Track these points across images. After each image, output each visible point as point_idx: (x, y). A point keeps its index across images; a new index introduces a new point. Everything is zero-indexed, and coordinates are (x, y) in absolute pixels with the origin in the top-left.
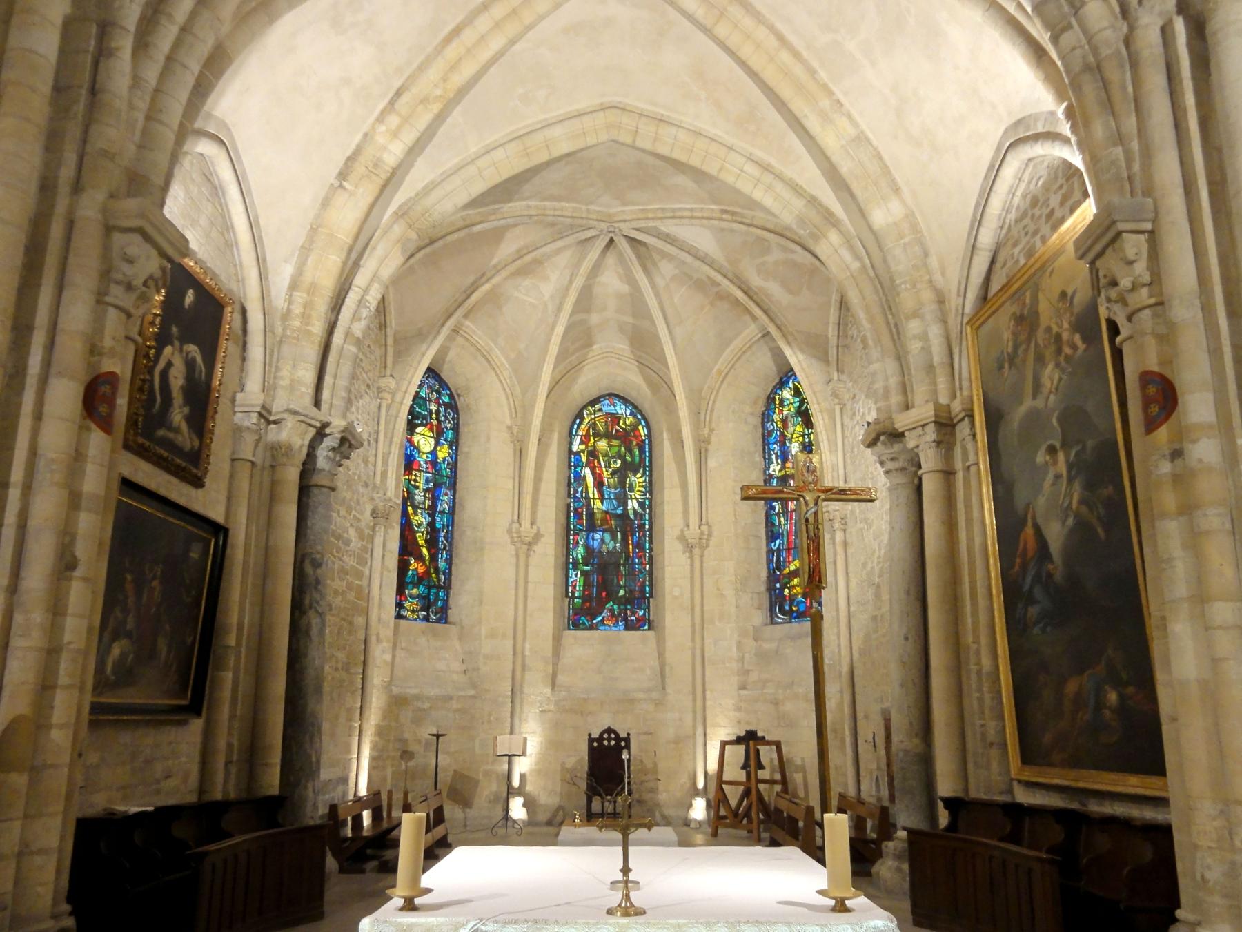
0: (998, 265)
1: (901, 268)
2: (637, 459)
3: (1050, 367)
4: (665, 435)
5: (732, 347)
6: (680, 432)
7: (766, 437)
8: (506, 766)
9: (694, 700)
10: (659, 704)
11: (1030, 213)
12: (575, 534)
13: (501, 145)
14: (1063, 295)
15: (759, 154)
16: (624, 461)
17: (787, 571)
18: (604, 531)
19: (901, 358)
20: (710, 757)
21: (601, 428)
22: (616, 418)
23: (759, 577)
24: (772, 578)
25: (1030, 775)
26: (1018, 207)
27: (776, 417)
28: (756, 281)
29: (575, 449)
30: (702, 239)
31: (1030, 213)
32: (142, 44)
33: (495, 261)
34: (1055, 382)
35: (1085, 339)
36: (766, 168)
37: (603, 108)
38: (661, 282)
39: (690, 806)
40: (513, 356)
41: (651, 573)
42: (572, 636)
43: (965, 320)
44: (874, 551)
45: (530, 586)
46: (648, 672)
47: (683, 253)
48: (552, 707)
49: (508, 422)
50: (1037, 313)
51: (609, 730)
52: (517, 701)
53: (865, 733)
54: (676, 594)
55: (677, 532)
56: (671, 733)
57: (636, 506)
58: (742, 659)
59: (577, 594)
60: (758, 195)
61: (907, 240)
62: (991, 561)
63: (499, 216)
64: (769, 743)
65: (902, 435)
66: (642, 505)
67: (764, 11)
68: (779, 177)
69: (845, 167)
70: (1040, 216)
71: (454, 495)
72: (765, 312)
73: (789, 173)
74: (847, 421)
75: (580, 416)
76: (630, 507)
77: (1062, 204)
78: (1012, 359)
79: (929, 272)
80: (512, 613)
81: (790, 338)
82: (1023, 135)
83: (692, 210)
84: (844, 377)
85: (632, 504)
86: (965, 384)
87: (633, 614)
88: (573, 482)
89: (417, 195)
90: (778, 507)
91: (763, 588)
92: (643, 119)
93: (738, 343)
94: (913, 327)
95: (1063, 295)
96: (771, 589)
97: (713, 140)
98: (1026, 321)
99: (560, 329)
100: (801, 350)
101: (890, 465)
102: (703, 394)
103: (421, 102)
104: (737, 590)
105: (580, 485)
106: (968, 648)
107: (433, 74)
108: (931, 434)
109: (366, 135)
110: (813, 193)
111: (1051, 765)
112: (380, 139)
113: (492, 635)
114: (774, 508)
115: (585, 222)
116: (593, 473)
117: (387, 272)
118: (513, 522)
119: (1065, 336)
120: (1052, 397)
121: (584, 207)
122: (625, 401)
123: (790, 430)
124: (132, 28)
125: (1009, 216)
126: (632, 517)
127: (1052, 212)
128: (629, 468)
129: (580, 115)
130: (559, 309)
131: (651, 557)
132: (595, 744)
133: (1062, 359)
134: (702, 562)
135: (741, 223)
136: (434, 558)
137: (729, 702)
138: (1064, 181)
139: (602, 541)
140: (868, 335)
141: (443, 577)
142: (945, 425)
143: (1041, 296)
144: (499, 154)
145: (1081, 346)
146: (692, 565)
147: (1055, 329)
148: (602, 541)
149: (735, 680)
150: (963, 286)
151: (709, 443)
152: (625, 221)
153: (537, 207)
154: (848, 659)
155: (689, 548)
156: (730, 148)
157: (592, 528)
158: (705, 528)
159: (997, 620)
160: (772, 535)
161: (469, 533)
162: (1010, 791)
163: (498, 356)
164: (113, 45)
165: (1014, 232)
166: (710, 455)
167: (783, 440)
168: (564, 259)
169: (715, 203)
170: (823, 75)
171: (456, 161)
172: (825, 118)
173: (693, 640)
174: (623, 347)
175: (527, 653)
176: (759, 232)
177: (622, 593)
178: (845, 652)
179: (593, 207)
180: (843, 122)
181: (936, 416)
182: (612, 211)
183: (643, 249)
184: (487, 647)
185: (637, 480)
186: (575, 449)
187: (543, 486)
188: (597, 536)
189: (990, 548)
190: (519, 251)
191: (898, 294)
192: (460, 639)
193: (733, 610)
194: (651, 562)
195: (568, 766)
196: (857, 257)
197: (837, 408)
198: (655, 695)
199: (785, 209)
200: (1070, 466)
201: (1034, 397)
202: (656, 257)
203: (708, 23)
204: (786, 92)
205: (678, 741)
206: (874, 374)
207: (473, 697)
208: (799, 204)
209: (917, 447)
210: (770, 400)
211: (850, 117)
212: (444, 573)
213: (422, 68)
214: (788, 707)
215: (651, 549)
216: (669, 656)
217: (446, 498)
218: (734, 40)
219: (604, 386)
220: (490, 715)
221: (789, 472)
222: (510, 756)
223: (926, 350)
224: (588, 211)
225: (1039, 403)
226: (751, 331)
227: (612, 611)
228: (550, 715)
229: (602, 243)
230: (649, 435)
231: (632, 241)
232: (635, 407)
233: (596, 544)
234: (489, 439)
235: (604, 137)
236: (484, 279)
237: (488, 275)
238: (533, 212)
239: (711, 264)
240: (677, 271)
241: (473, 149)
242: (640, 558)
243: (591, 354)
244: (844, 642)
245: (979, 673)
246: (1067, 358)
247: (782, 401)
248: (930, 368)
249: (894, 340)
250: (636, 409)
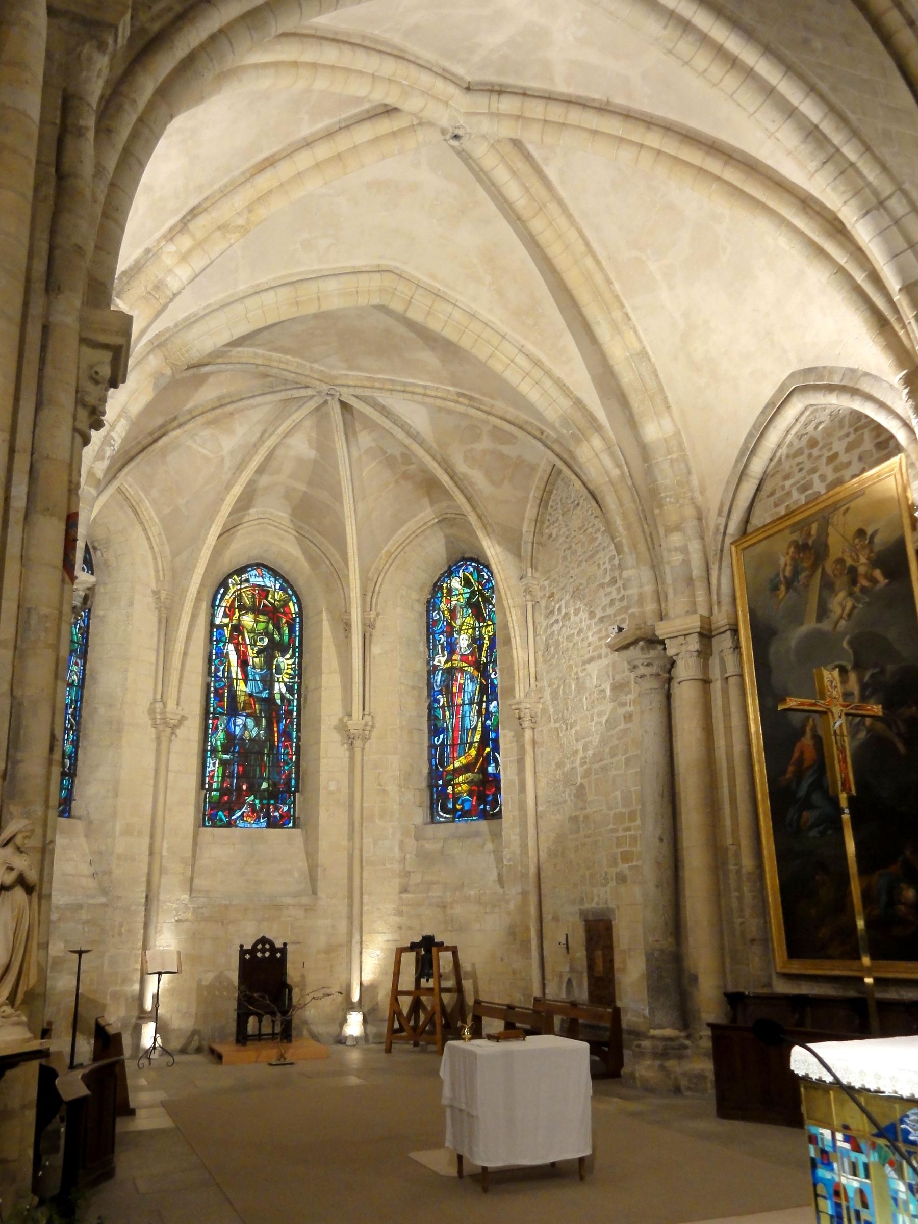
0: (763, 494)
1: (668, 482)
2: (286, 638)
3: (842, 595)
4: (325, 615)
5: (404, 529)
6: (348, 612)
7: (430, 626)
8: (137, 987)
9: (351, 906)
10: (309, 909)
11: (807, 452)
12: (215, 718)
13: (272, 288)
14: (861, 533)
15: (531, 348)
16: (272, 640)
17: (451, 767)
18: (247, 716)
19: (656, 566)
20: (372, 963)
22: (264, 592)
23: (420, 772)
24: (434, 775)
25: (796, 967)
26: (791, 445)
27: (443, 606)
28: (462, 467)
29: (218, 621)
30: (417, 416)
31: (807, 452)
32: (104, 130)
33: (190, 405)
34: (848, 609)
35: (886, 575)
36: (537, 363)
37: (380, 271)
38: (355, 453)
39: (345, 1020)
40: (167, 511)
41: (298, 764)
42: (208, 833)
43: (728, 540)
44: (576, 752)
45: (171, 776)
46: (296, 875)
47: (396, 428)
48: (189, 915)
49: (153, 585)
50: (826, 546)
51: (263, 940)
52: (154, 908)
53: (556, 935)
54: (332, 787)
55: (334, 721)
56: (321, 941)
57: (284, 690)
58: (403, 860)
59: (215, 786)
60: (525, 388)
61: (674, 456)
62: (757, 768)
63: (226, 360)
64: (447, 949)
65: (662, 642)
66: (290, 689)
67: (577, 215)
68: (548, 373)
69: (627, 377)
70: (819, 457)
71: (84, 665)
72: (469, 499)
73: (558, 372)
74: (540, 619)
75: (224, 584)
76: (276, 690)
77: (848, 450)
78: (790, 584)
79: (691, 490)
81: (490, 530)
82: (810, 381)
83: (425, 387)
84: (537, 575)
85: (279, 688)
86: (726, 600)
87: (277, 809)
88: (214, 659)
89: (176, 326)
90: (442, 700)
91: (424, 784)
92: (421, 291)
93: (411, 525)
95: (861, 533)
96: (431, 786)
97: (487, 325)
98: (810, 551)
99: (237, 490)
100: (499, 543)
101: (642, 670)
102: (370, 575)
103: (219, 228)
104: (400, 786)
105: (222, 663)
106: (727, 849)
107: (239, 200)
108: (694, 644)
109: (148, 251)
110: (579, 395)
111: (830, 958)
112: (168, 260)
113: (128, 831)
114: (438, 701)
116: (237, 650)
117: (135, 408)
118: (155, 701)
119: (862, 570)
120: (843, 623)
121: (308, 364)
122: (275, 573)
123: (459, 621)
124: (95, 106)
125: (780, 451)
126: (279, 702)
127: (833, 458)
130: (240, 468)
131: (298, 747)
132: (248, 956)
133: (857, 589)
134: (362, 756)
135: (478, 409)
137: (389, 907)
138: (851, 430)
139: (245, 726)
140: (624, 541)
141: (68, 762)
142: (706, 635)
143: (831, 530)
144: (269, 298)
145: (883, 581)
146: (352, 758)
147: (849, 562)
148: (245, 726)
149: (396, 883)
150: (726, 509)
151: (374, 628)
152: (348, 386)
153: (263, 356)
154: (536, 860)
155: (350, 740)
156: (504, 337)
157: (233, 711)
158: (368, 718)
159: (762, 823)
160: (435, 729)
161: (102, 711)
162: (769, 985)
163: (147, 508)
164: (82, 123)
165: (786, 466)
166: (374, 639)
167: (450, 631)
169: (454, 385)
170: (617, 286)
171: (222, 296)
172: (616, 329)
173: (351, 838)
174: (283, 515)
175: (164, 853)
176: (498, 422)
177: (265, 786)
178: (532, 853)
179: (316, 366)
180: (630, 336)
181: (701, 627)
182: (334, 373)
183: (348, 416)
184: (120, 848)
185: (285, 662)
186: (218, 621)
187: (189, 661)
188: (240, 721)
189: (755, 756)
190: (220, 398)
191: (661, 507)
192: (86, 836)
193: (396, 807)
194: (298, 753)
195: (204, 983)
196: (618, 466)
197: (529, 605)
198: (305, 900)
199: (551, 407)
200: (863, 687)
201: (819, 619)
202: (358, 426)
203: (526, 214)
204: (584, 296)
205: (330, 950)
206: (628, 580)
207: (105, 905)
208: (565, 404)
209: (677, 655)
210: (437, 587)
211: (636, 332)
212: (70, 758)
213: (226, 192)
214: (458, 910)
215: (298, 738)
216: (324, 857)
217: (75, 668)
218: (546, 237)
219: (255, 554)
220: (121, 925)
221: (456, 664)
223: (686, 563)
224: (312, 368)
225: (826, 626)
226: (427, 513)
227: (253, 806)
228: (187, 924)
229: (312, 405)
230: (300, 613)
231: (344, 405)
232: (285, 581)
233: (238, 731)
234: (131, 604)
235: (376, 301)
236: (175, 424)
237: (182, 419)
238: (260, 361)
239: (422, 443)
240: (373, 444)
241: (242, 287)
242: (286, 747)
243: (246, 520)
244: (531, 842)
245: (738, 872)
246: (864, 590)
247: (450, 590)
248: (690, 581)
249: (649, 549)
250: (287, 584)
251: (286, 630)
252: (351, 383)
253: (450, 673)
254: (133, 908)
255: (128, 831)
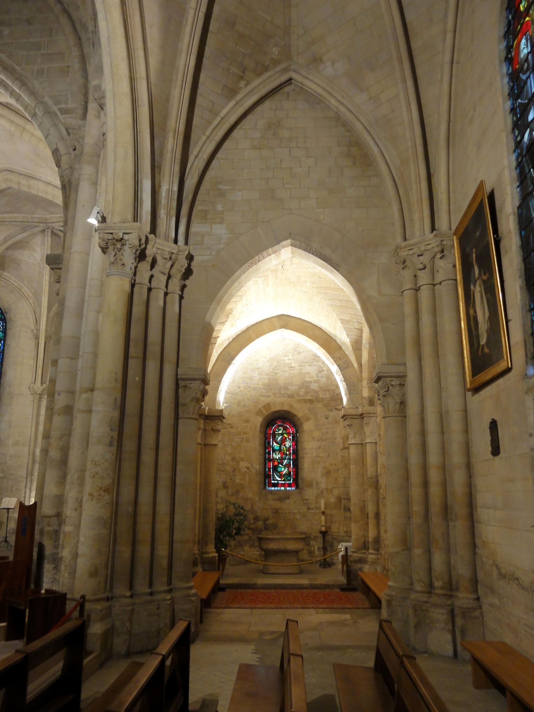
40: (33, 291)
80: (30, 432)
113: (16, 444)
115: (30, 224)
118: (32, 383)
152: (53, 222)
161: (7, 389)
168: (38, 240)
182: (48, 217)
190: (5, 238)
220: (12, 487)
222: (8, 509)
224: (32, 218)
234: (19, 337)
252: (55, 221)
254: (19, 479)
255: (16, 444)
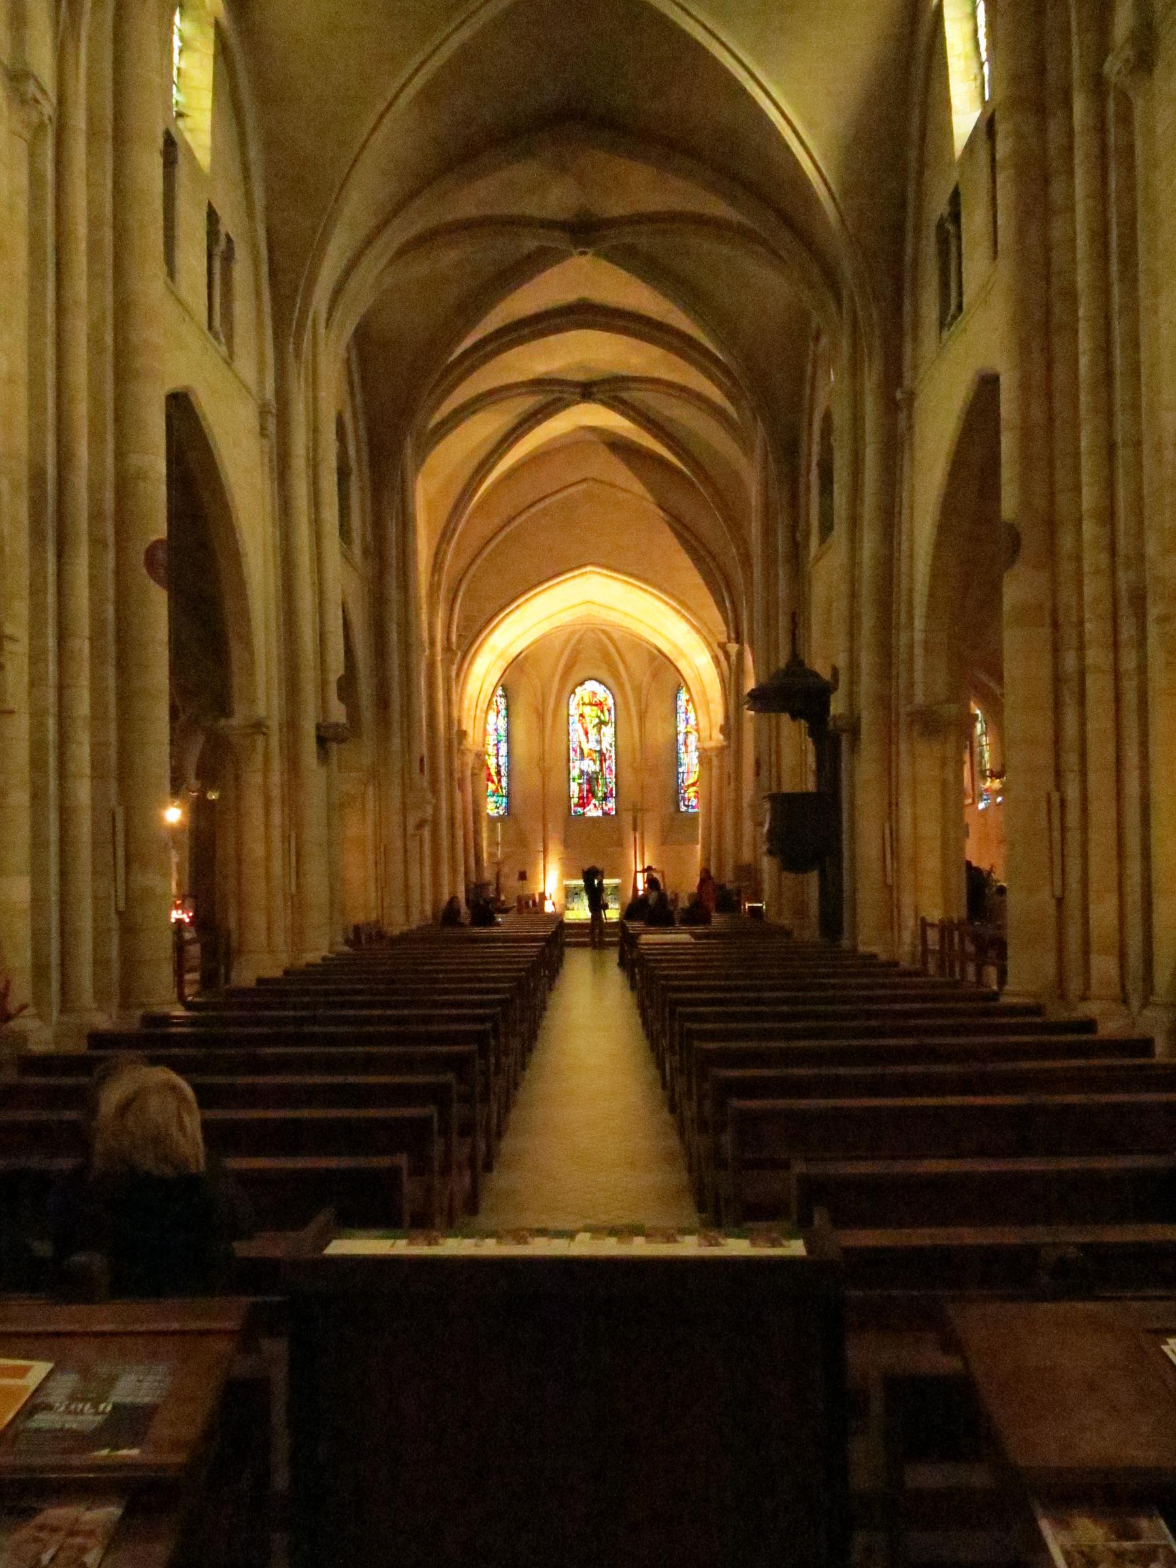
21: (587, 701)
22: (594, 694)
32: (457, 682)
75: (573, 692)
90: (683, 748)
94: (712, 706)
122: (601, 682)
128: (602, 723)
129: (573, 606)
136: (499, 781)
177: (600, 794)
233: (585, 769)
251: (606, 713)
253: (687, 733)
